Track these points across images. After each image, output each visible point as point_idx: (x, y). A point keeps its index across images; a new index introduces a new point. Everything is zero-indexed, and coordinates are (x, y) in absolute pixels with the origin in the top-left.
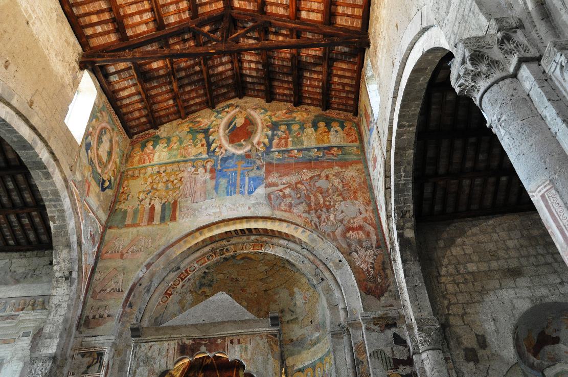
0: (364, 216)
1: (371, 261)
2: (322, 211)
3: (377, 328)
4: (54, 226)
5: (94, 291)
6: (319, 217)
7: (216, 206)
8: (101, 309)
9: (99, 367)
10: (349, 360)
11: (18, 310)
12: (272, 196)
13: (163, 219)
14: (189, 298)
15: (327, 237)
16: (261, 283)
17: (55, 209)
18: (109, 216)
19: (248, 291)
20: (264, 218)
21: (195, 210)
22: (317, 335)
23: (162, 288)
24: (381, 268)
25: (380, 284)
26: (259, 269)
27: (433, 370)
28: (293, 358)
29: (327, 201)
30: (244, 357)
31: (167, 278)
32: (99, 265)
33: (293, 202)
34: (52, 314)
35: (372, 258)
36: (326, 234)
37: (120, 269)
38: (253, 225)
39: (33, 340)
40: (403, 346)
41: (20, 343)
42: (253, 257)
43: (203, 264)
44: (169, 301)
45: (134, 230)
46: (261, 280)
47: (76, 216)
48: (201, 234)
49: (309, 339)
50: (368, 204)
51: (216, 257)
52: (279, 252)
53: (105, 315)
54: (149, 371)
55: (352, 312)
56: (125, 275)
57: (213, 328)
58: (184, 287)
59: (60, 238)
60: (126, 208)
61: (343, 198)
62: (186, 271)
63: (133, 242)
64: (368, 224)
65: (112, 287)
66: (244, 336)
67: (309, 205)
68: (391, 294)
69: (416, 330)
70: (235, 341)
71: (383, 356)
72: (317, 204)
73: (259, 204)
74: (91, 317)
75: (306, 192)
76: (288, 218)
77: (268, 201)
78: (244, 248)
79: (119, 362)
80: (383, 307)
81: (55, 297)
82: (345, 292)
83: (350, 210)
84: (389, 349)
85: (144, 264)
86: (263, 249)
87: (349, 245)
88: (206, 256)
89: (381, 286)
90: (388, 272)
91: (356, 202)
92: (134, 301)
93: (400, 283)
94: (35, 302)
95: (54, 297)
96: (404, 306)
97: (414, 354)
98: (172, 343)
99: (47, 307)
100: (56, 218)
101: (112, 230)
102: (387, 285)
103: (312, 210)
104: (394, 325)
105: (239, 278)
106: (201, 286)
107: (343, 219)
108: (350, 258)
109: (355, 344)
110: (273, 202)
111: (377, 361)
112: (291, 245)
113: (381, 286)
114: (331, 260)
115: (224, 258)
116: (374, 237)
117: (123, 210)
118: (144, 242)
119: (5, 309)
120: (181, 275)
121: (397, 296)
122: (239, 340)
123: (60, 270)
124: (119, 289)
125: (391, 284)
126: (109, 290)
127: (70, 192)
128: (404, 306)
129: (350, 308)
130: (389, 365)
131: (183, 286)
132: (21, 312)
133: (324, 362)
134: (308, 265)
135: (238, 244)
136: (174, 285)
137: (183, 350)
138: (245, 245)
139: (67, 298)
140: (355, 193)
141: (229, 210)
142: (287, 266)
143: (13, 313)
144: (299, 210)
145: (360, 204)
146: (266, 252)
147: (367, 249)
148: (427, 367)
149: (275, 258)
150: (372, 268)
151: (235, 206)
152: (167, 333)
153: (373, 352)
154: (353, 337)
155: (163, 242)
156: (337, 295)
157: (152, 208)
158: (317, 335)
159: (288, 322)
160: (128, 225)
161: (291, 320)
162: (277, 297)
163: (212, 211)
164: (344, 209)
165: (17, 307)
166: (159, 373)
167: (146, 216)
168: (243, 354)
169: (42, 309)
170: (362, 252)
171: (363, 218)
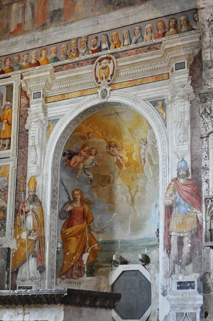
11: (159, 36)
39: (192, 72)
41: (176, 78)
81: (204, 10)
94: (176, 22)
95: (201, 11)
99: (194, 27)
119: (143, 38)
132: (164, 38)
143: (154, 41)
165: (156, 32)
169: (189, 30)
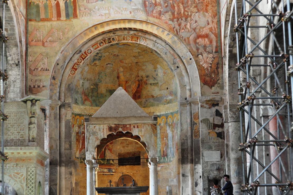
0: (210, 27)
1: (210, 62)
2: (182, 20)
3: (207, 106)
4: (7, 34)
5: (30, 70)
6: (180, 25)
7: (106, 8)
8: (37, 82)
9: (45, 117)
10: (189, 120)
12: (147, 3)
13: (67, 15)
14: (86, 69)
15: (184, 42)
16: (134, 58)
17: (9, 25)
18: (26, 9)
19: (124, 62)
20: (141, 22)
21: (90, 10)
22: (170, 98)
23: (71, 65)
24: (216, 67)
25: (213, 79)
26: (134, 50)
27: (232, 132)
28: (153, 108)
29: (187, 12)
30: (140, 134)
31: (73, 58)
32: (29, 50)
33: (162, 10)
34: (12, 86)
35: (211, 60)
36: (183, 39)
37: (44, 54)
38: (133, 26)
40: (220, 117)
42: (131, 45)
43: (96, 48)
44: (76, 74)
45: (48, 24)
46: (134, 56)
47: (18, 25)
48: (96, 29)
49: (165, 98)
50: (214, 17)
51: (105, 44)
52: (150, 44)
53: (41, 86)
54: (96, 138)
55: (194, 94)
56: (49, 59)
57: (125, 120)
58: (85, 63)
59: (11, 41)
60: (37, 3)
61: (198, 9)
62: (85, 53)
63: (50, 33)
64: (212, 33)
65: (41, 67)
66: (140, 124)
67: (173, 14)
68: (219, 85)
69: (229, 110)
70: (136, 126)
71: (208, 122)
72: (179, 13)
73: (137, 9)
74: (32, 86)
75: (171, 2)
76: (158, 23)
77: (144, 8)
78: (125, 38)
79: (53, 114)
80: (213, 93)
81: (12, 76)
82: (192, 81)
83: (201, 20)
84: (212, 118)
85: (60, 52)
86: (138, 41)
87: (198, 49)
88: (99, 42)
89: (214, 80)
90: (220, 70)
91: (207, 14)
92: (55, 75)
93: (225, 79)
95: (10, 76)
96: (225, 94)
97: (225, 122)
98: (105, 125)
100: (9, 29)
101: (33, 23)
102: (217, 79)
103: (175, 18)
104: (217, 105)
105: (119, 54)
106: (94, 60)
107: (195, 28)
108: (197, 59)
109: (193, 114)
110: (147, 8)
111: (204, 124)
112: (159, 41)
113: (214, 80)
114: (185, 58)
115: (111, 45)
116: (214, 44)
117: (35, 4)
118: (56, 34)
120: (82, 55)
121: (222, 87)
122: (138, 126)
123: (12, 60)
124: (46, 69)
125: (220, 79)
126: (40, 69)
127: (16, 12)
128: (225, 94)
129: (193, 91)
130: (210, 127)
131: (84, 63)
133: (174, 116)
134: (169, 56)
135: (121, 35)
136: (78, 62)
137: (110, 129)
138: (126, 36)
139: (19, 77)
140: (207, 6)
141: (116, 12)
142: (154, 52)
144: (166, 17)
145: (209, 16)
146: (140, 43)
147: (209, 53)
148: (230, 130)
149: (146, 47)
150: (210, 67)
151: (120, 10)
152: (102, 121)
153: (203, 120)
154: (193, 109)
155: (70, 34)
156: (186, 80)
157: (58, 5)
158: (170, 98)
159: (151, 84)
160: (43, 19)
161: (154, 84)
162: (144, 67)
163: (103, 12)
164: (197, 19)
166: (101, 139)
167: (55, 12)
168: (140, 133)
170: (205, 55)
171: (209, 28)
